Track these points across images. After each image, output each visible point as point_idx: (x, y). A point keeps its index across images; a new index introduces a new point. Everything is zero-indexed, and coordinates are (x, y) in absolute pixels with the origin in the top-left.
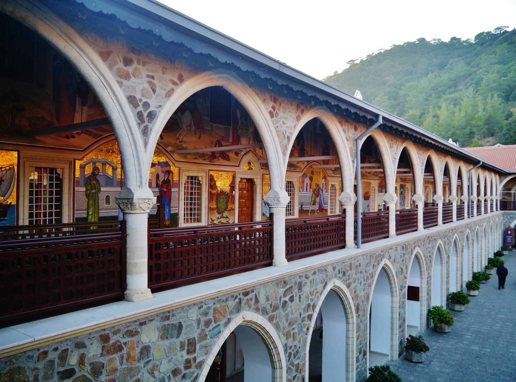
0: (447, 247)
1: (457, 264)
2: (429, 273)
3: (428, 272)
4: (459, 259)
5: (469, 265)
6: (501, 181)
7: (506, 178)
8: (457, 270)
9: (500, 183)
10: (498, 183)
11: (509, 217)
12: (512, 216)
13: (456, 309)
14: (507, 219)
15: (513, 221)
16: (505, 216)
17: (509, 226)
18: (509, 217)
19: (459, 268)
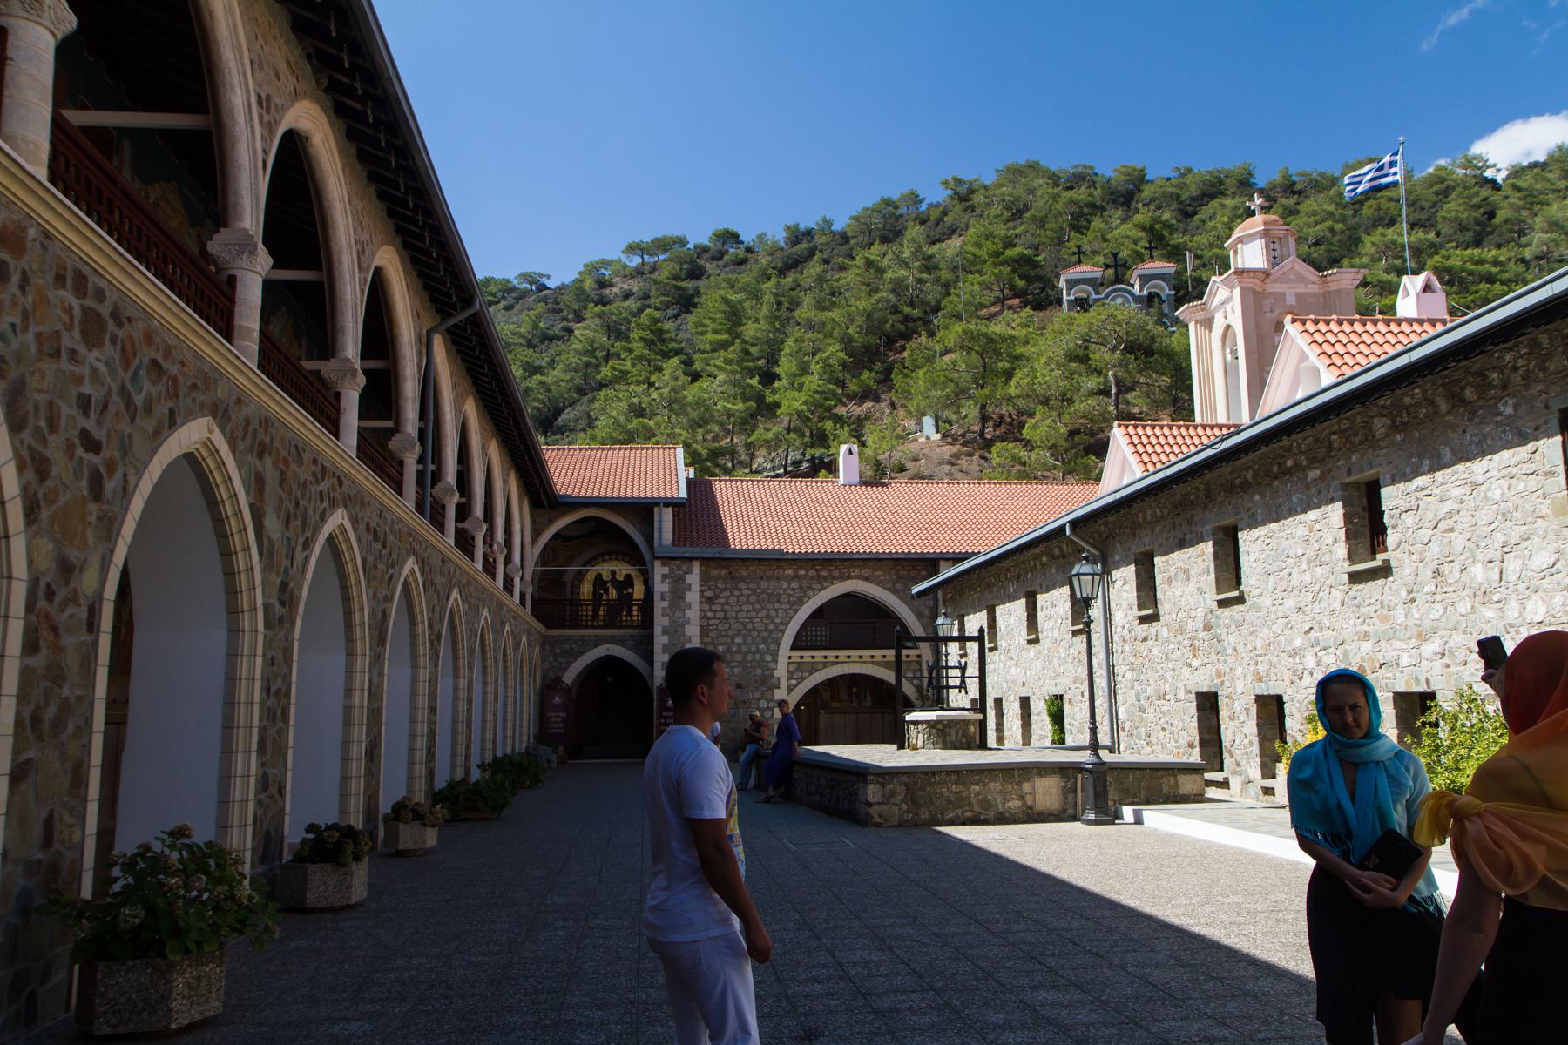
0: (272, 524)
1: (349, 692)
2: (66, 569)
3: (46, 547)
4: (363, 662)
5: (412, 736)
6: (536, 534)
7: (551, 521)
8: (347, 723)
9: (535, 538)
10: (528, 539)
11: (558, 651)
12: (566, 647)
13: (312, 899)
14: (551, 658)
15: (569, 664)
16: (547, 647)
17: (558, 679)
18: (558, 651)
19: (360, 716)
